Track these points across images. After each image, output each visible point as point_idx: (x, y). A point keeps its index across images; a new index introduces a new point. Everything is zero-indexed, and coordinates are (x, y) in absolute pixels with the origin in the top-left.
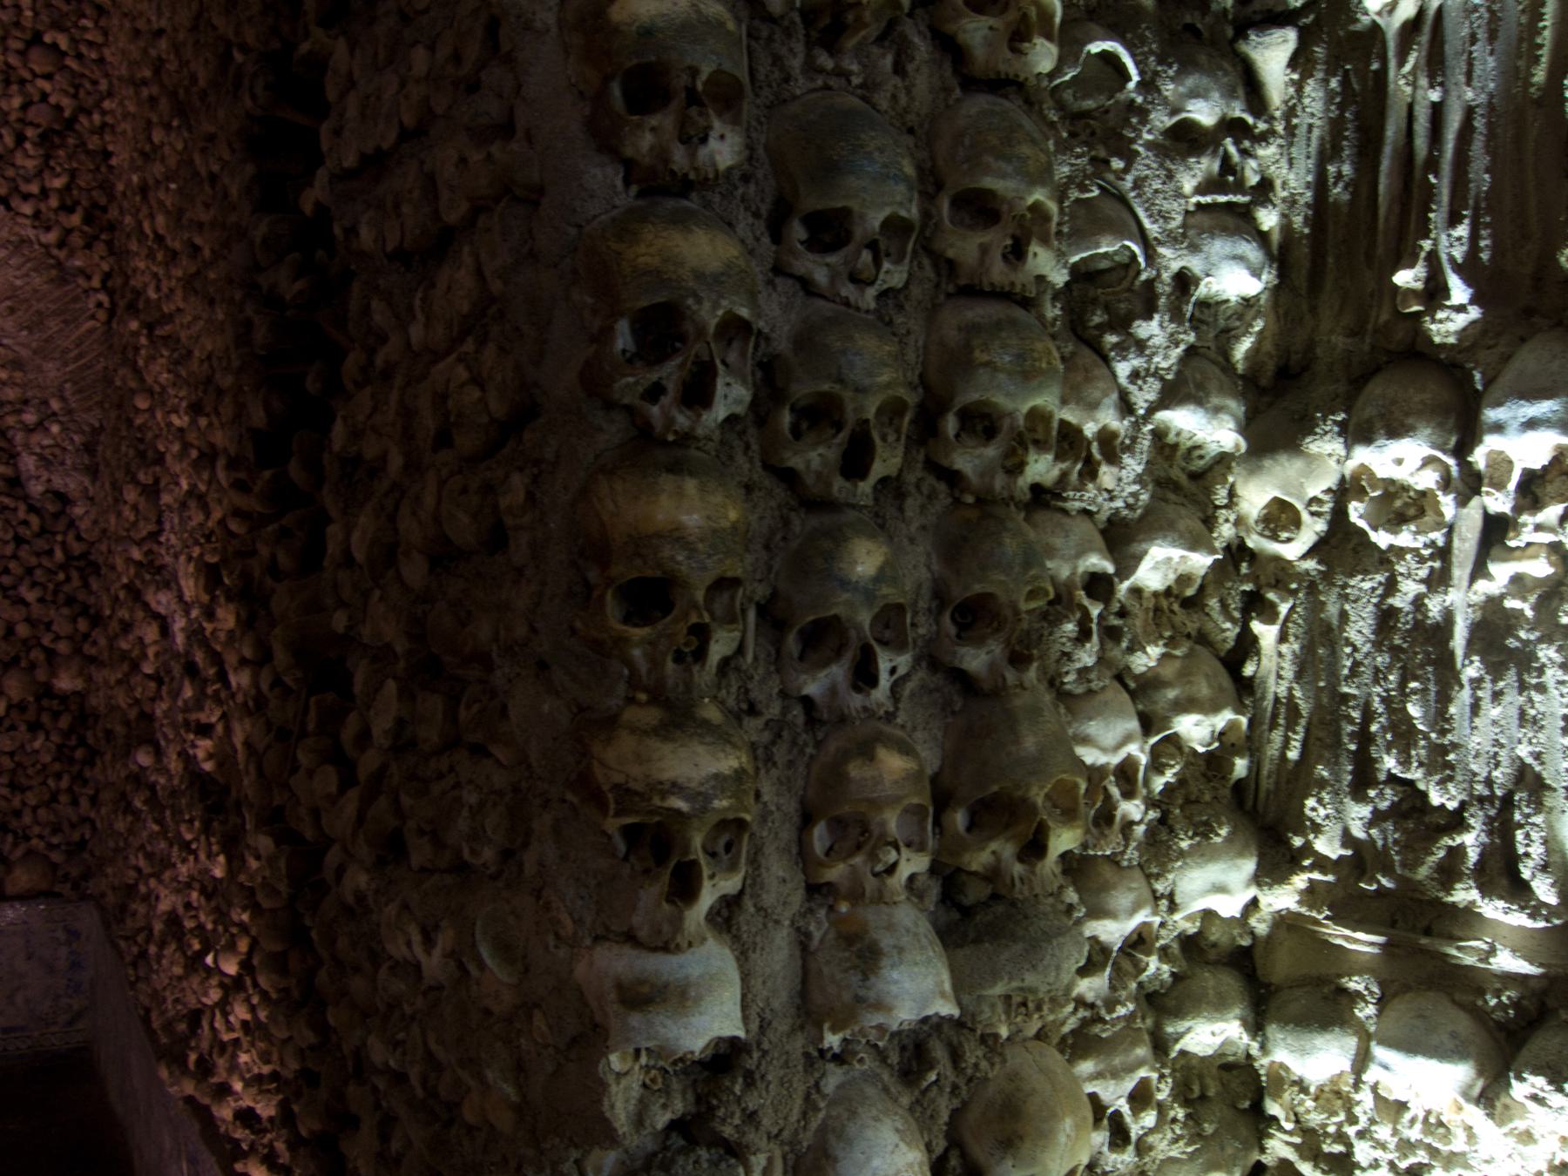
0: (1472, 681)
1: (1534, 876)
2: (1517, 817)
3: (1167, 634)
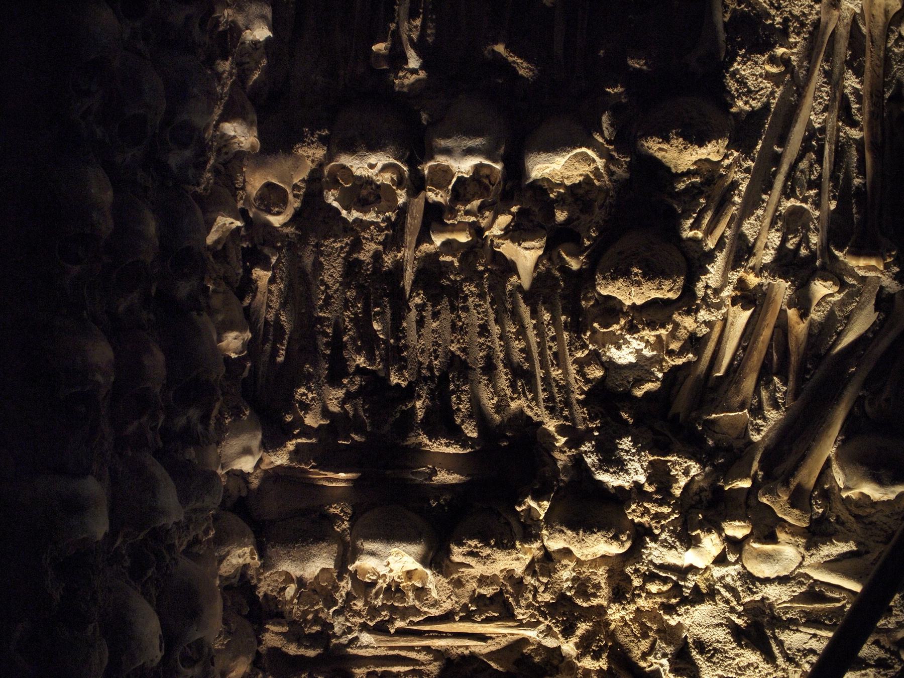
0: (417, 306)
1: (463, 422)
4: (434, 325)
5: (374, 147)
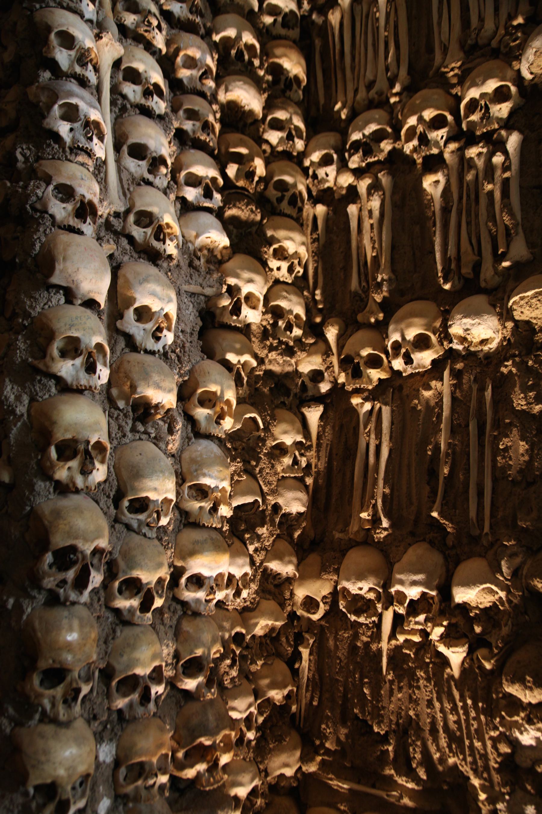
0: (389, 680)
1: (417, 767)
2: (410, 741)
3: (265, 654)
4: (400, 696)
5: (360, 577)
